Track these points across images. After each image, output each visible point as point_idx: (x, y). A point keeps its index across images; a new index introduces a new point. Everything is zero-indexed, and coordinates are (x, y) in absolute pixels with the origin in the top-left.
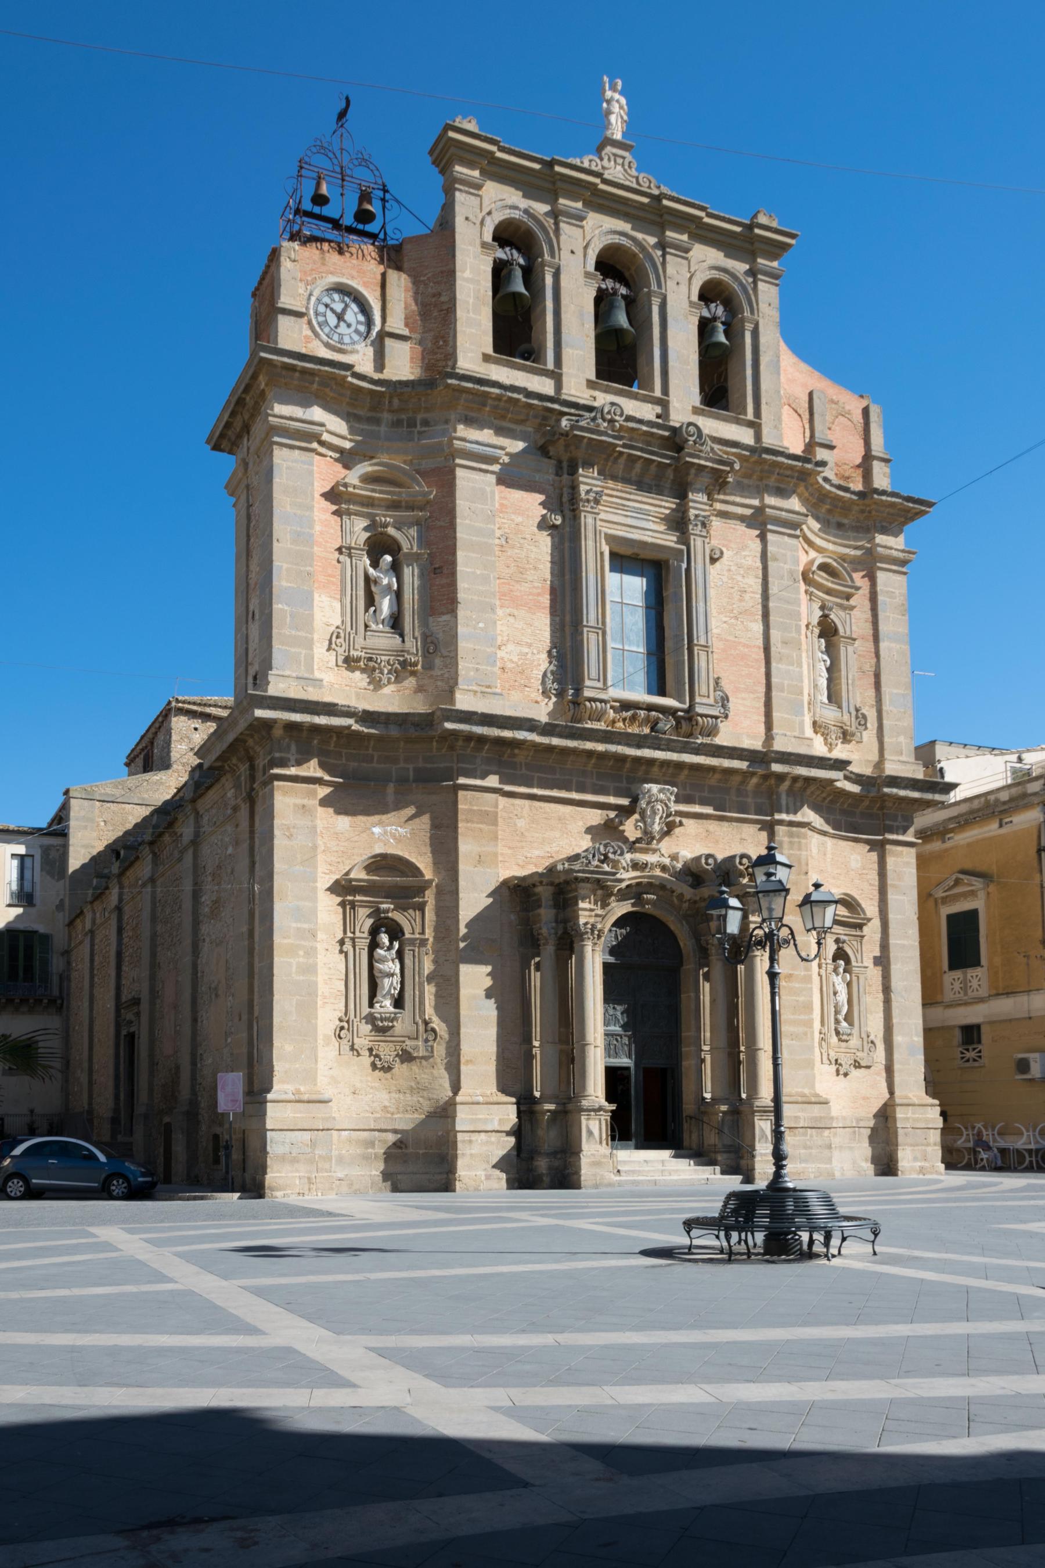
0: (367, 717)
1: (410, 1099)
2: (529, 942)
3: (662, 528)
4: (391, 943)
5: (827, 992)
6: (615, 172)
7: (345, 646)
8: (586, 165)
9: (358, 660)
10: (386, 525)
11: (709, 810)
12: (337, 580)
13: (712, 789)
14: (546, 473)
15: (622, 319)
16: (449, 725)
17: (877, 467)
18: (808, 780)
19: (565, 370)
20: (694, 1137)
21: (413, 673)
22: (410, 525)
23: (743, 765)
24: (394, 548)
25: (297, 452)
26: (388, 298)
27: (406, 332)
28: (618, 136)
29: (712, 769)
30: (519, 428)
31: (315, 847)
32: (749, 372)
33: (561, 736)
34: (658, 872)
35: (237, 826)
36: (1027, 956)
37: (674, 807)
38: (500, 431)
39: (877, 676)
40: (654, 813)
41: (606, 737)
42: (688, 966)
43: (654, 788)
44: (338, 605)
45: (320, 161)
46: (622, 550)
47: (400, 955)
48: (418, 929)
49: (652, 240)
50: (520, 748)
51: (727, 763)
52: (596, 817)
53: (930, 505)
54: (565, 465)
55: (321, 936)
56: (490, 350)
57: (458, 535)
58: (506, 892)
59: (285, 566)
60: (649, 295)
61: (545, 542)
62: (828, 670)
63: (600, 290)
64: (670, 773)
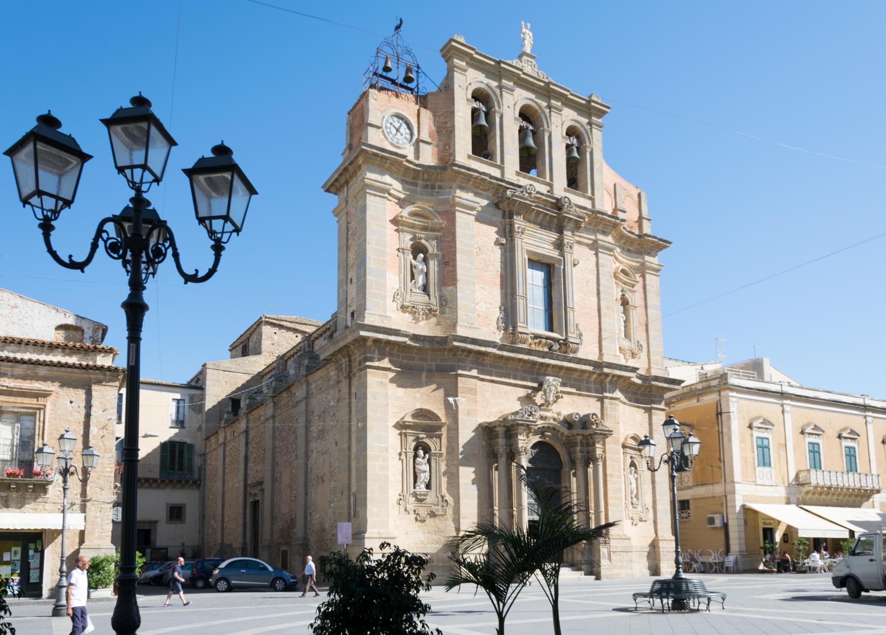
0: (415, 338)
1: (435, 537)
2: (492, 456)
3: (552, 248)
4: (425, 454)
5: (627, 483)
6: (528, 69)
7: (401, 300)
8: (514, 64)
9: (407, 307)
10: (421, 239)
11: (574, 390)
12: (397, 265)
13: (575, 380)
14: (498, 218)
15: (531, 142)
16: (455, 344)
17: (645, 223)
18: (619, 377)
19: (506, 165)
20: (570, 556)
21: (435, 315)
22: (433, 239)
23: (590, 368)
24: (424, 250)
25: (378, 198)
26: (421, 122)
27: (429, 140)
28: (529, 51)
29: (576, 370)
30: (485, 193)
31: (387, 404)
32: (589, 173)
33: (507, 351)
34: (552, 421)
35: (339, 391)
36: (712, 466)
37: (560, 389)
38: (476, 194)
39: (647, 326)
40: (551, 391)
41: (529, 352)
42: (565, 469)
43: (551, 379)
44: (397, 278)
45: (387, 50)
46: (533, 258)
47: (429, 461)
48: (438, 448)
49: (544, 104)
51: (583, 367)
52: (522, 392)
53: (670, 243)
54: (507, 213)
55: (390, 451)
56: (471, 153)
57: (458, 246)
58: (480, 429)
59: (373, 257)
60: (543, 131)
61: (497, 252)
62: (625, 322)
63: (521, 127)
64: (557, 371)
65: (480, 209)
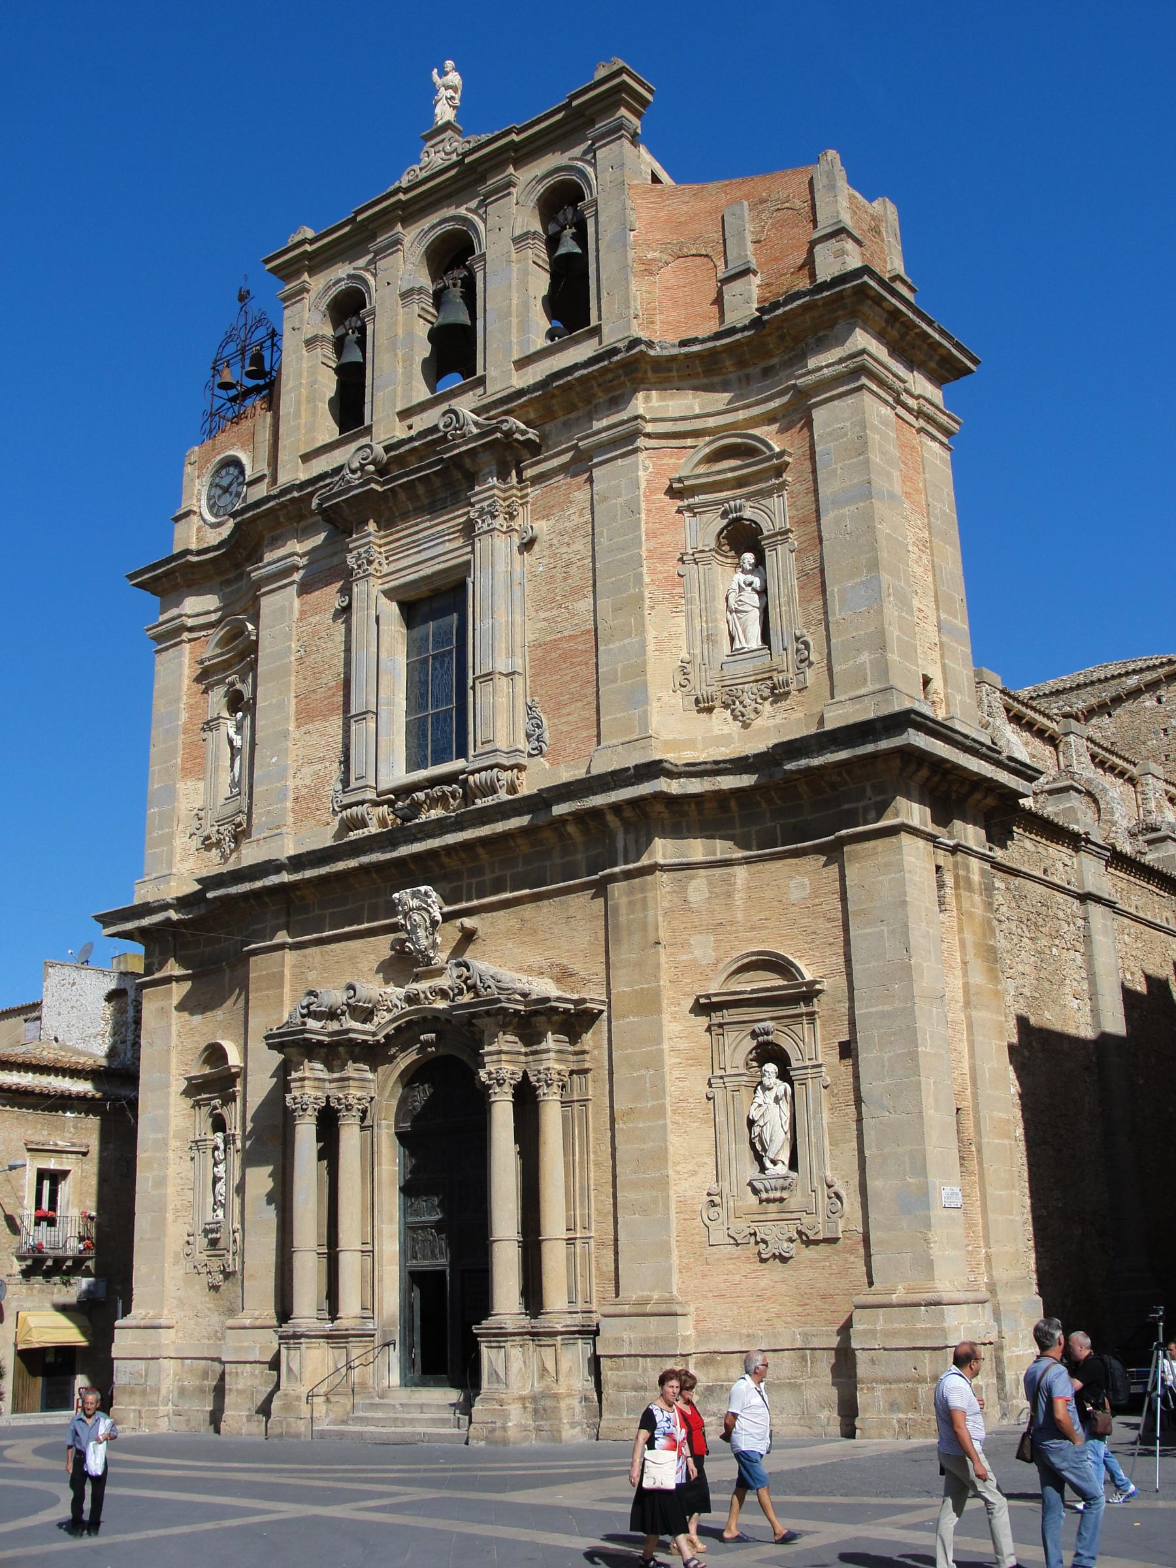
23: (523, 821)
46: (411, 596)
50: (299, 889)
52: (382, 947)
55: (174, 1143)
65: (305, 561)
